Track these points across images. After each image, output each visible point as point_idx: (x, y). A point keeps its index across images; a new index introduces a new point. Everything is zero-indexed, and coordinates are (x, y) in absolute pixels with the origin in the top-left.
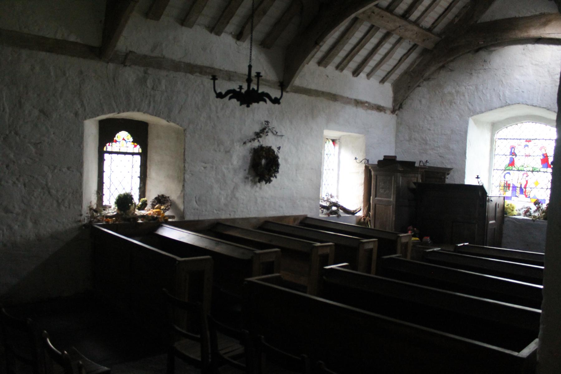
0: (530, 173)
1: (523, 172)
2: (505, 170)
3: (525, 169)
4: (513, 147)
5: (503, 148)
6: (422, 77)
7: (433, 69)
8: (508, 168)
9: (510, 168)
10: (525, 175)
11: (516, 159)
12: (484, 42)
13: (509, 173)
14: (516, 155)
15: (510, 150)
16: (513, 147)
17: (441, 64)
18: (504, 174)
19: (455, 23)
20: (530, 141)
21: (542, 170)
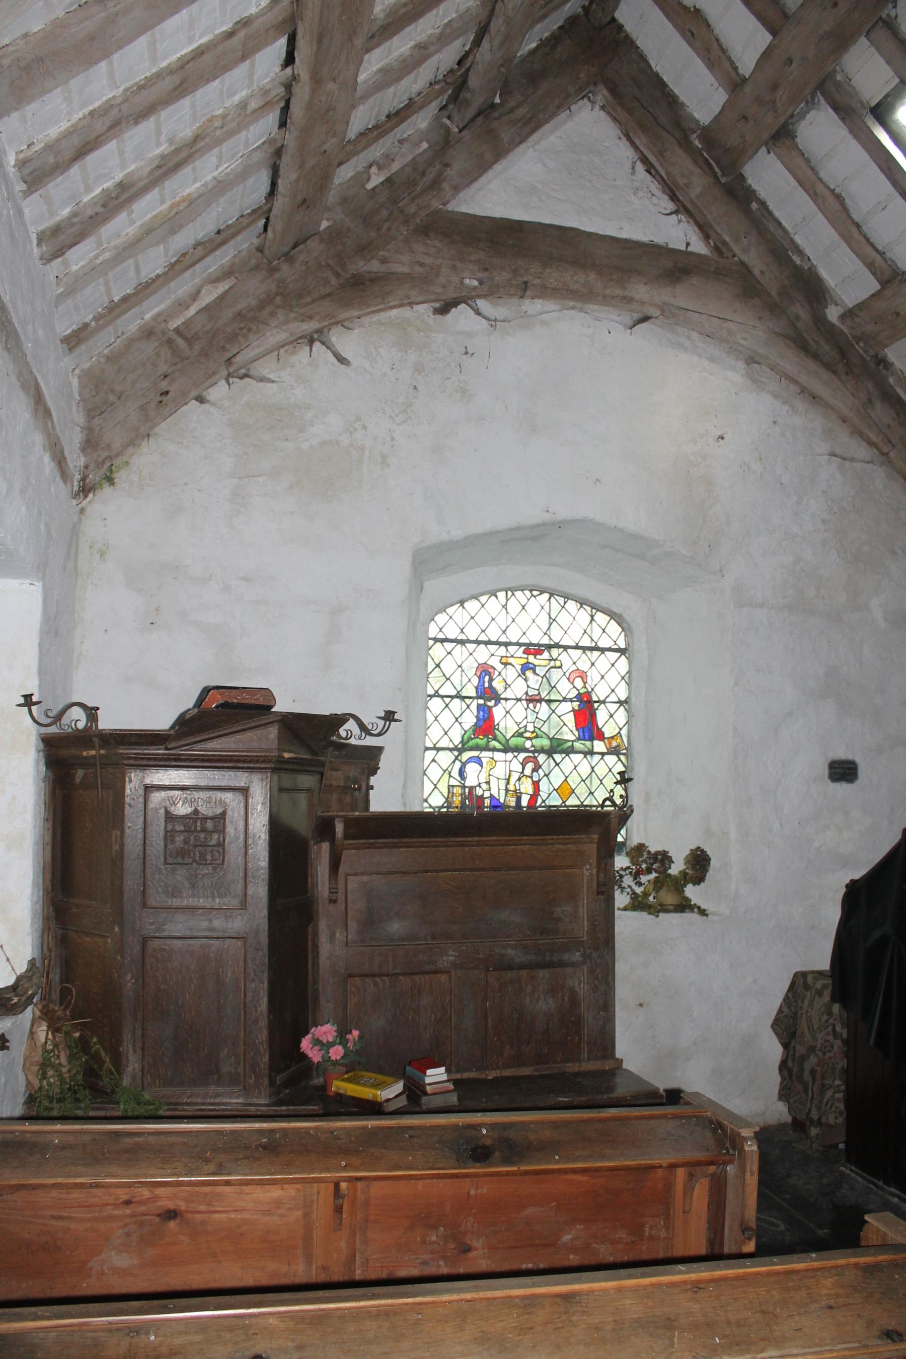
0: (542, 758)
1: (522, 756)
2: (460, 750)
3: (528, 744)
4: (484, 670)
5: (454, 669)
6: (229, 361)
7: (274, 336)
8: (471, 743)
9: (481, 741)
10: (530, 766)
11: (498, 713)
12: (481, 283)
13: (478, 761)
14: (498, 699)
15: (475, 681)
16: (484, 670)
17: (312, 325)
18: (458, 765)
19: (370, 186)
20: (539, 652)
21: (578, 745)
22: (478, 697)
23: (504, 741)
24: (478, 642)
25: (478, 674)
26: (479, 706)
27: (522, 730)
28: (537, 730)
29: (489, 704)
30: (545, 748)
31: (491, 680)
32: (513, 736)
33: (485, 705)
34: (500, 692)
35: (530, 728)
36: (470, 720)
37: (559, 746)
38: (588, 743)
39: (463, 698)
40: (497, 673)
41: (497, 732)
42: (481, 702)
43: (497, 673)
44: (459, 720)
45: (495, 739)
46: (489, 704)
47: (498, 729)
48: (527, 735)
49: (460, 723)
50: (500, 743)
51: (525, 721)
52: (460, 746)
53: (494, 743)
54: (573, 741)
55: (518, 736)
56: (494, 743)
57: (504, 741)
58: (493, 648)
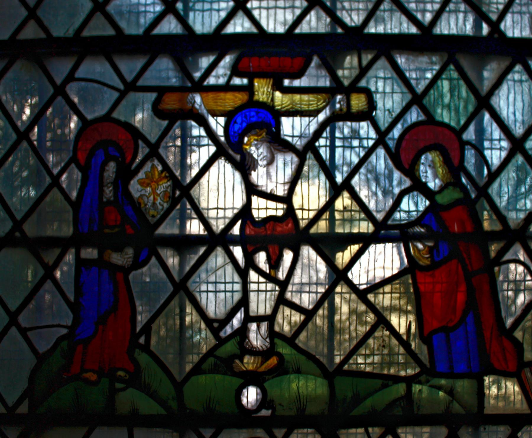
15: (71, 180)
22: (76, 242)
23: (166, 390)
24: (81, 47)
25: (82, 157)
26: (81, 263)
27: (230, 347)
28: (285, 350)
29: (117, 259)
30: (312, 409)
31: (126, 174)
32: (197, 370)
33: (101, 262)
34: (152, 215)
35: (256, 337)
36: (55, 313)
37: (358, 399)
38: (463, 386)
39: (38, 246)
40: (143, 151)
41: (143, 358)
42: (90, 253)
43: (143, 151)
44: (23, 320)
45: (136, 380)
46: (117, 259)
47: (146, 348)
48: (249, 363)
49: (23, 331)
50: (153, 395)
51: (239, 316)
52: (23, 409)
53: (130, 399)
54: (409, 380)
55: (214, 370)
56: (130, 399)
57: (166, 390)
58: (130, 66)
